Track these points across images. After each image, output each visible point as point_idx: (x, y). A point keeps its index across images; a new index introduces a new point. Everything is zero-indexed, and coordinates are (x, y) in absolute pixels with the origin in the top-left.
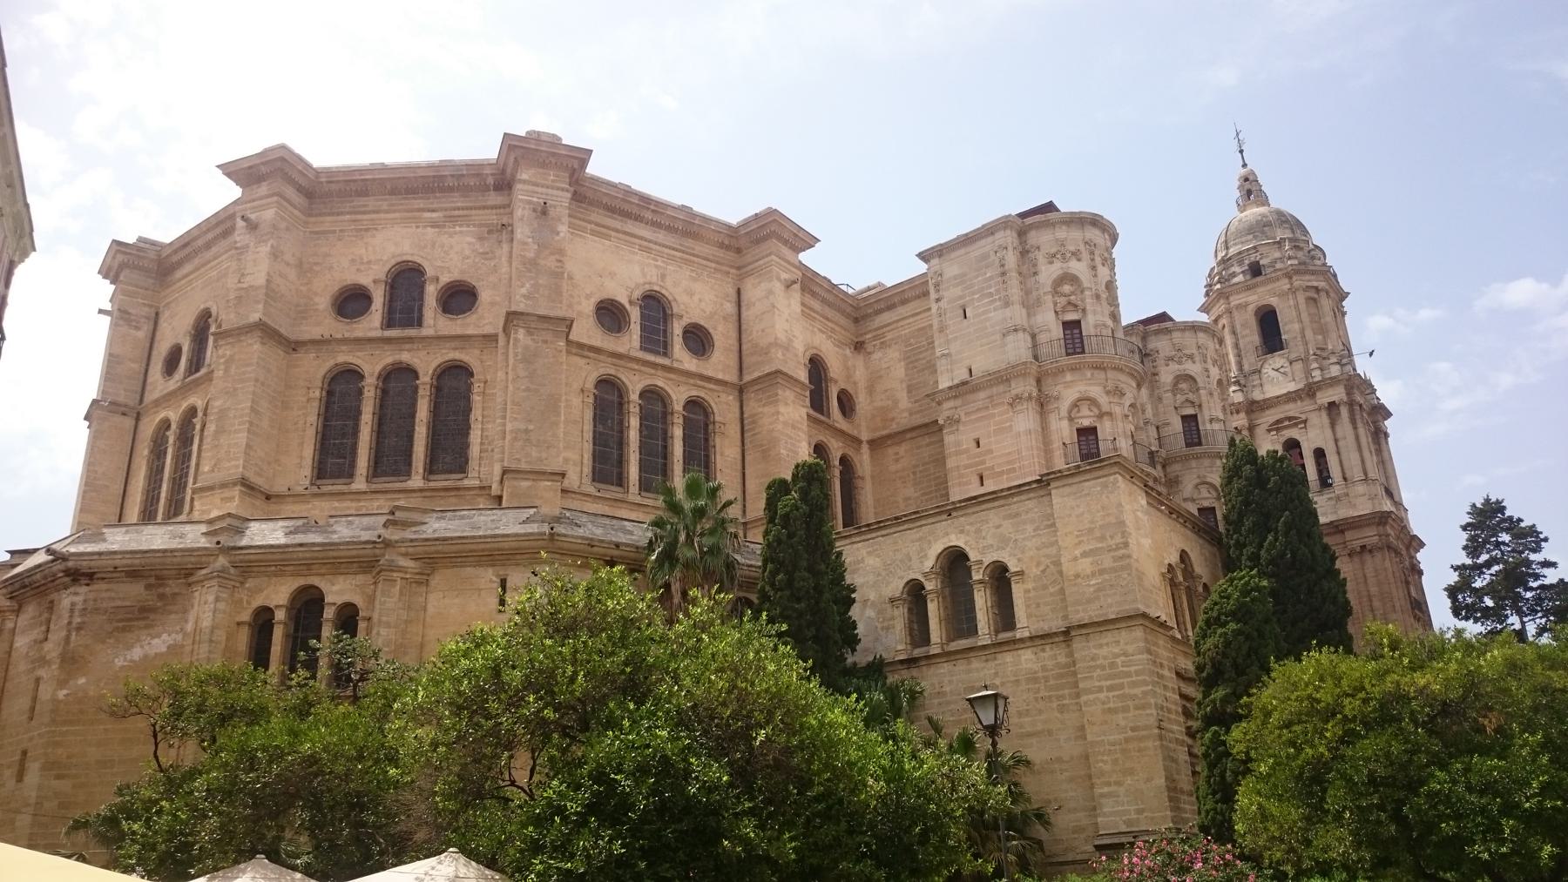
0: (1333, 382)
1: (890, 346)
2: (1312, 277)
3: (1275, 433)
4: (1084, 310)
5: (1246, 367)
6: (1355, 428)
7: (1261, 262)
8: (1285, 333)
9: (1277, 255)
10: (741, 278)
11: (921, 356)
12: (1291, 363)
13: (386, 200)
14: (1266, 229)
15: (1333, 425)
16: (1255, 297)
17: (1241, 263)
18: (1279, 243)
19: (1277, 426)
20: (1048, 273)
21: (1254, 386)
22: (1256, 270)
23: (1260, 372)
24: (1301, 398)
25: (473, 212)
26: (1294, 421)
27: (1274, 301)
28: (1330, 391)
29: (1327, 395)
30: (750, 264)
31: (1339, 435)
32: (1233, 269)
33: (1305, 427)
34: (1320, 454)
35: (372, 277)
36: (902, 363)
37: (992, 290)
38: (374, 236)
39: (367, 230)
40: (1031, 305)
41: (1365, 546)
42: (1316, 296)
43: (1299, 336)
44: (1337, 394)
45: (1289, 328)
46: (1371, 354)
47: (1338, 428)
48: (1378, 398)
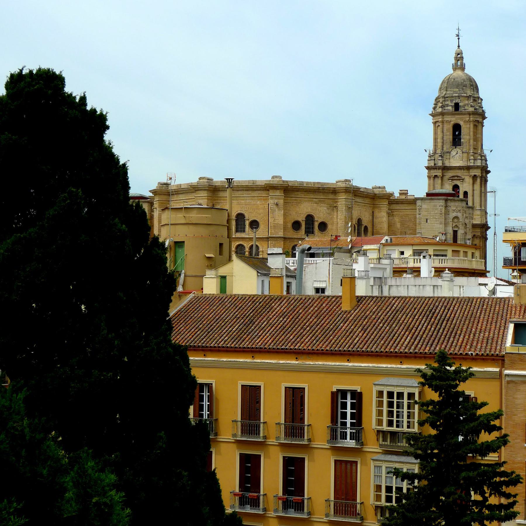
0: (477, 167)
1: (396, 216)
2: (478, 116)
3: (451, 181)
4: (459, 228)
5: (445, 149)
6: (481, 187)
7: (460, 104)
8: (463, 139)
9: (467, 102)
10: (374, 208)
11: (406, 223)
12: (463, 153)
13: (303, 193)
14: (464, 88)
15: (473, 184)
16: (454, 119)
17: (451, 101)
18: (468, 97)
19: (452, 178)
20: (452, 215)
21: (446, 158)
22: (457, 106)
23: (450, 153)
24: (464, 170)
25: (326, 200)
27: (461, 123)
28: (475, 171)
29: (473, 171)
30: (377, 205)
32: (447, 103)
33: (463, 182)
35: (301, 218)
36: (399, 223)
37: (437, 217)
38: (301, 205)
39: (299, 203)
40: (446, 224)
41: (475, 235)
42: (477, 124)
43: (468, 142)
44: (478, 173)
46: (491, 151)
47: (475, 185)
48: (486, 164)
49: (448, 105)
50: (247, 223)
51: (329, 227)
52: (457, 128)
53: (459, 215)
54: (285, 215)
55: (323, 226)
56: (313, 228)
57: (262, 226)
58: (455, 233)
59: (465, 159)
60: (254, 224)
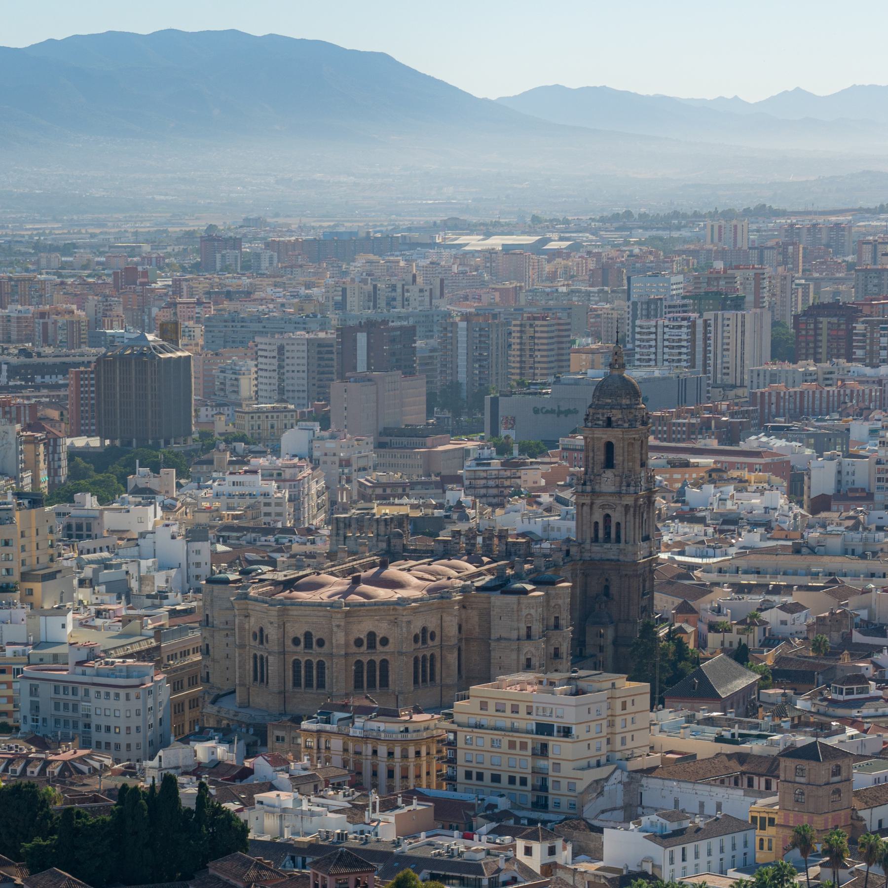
9: (620, 416)
17: (603, 415)
19: (603, 507)
26: (610, 507)
27: (614, 441)
31: (628, 519)
34: (618, 524)
45: (618, 459)
49: (598, 419)
50: (314, 640)
51: (391, 641)
52: (609, 447)
53: (533, 612)
54: (347, 635)
55: (385, 641)
56: (375, 643)
57: (327, 644)
58: (529, 628)
59: (617, 484)
60: (321, 643)
